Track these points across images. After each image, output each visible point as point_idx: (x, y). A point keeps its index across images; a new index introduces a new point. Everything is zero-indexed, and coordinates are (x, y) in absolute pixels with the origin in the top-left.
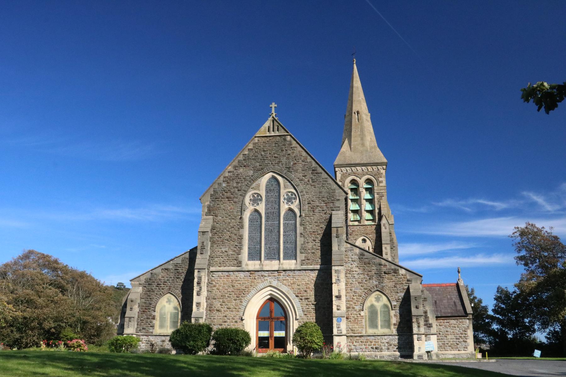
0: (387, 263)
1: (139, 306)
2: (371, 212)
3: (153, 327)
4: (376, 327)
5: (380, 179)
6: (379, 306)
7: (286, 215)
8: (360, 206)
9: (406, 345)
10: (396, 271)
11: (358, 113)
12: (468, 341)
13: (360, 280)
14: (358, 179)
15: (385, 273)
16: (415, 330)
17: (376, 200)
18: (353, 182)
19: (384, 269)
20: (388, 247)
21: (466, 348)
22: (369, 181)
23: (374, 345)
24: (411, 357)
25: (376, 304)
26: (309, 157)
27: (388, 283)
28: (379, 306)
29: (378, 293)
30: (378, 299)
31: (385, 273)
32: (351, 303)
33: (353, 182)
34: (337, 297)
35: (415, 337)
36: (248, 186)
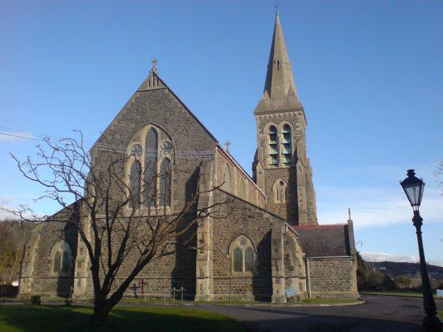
0: (252, 208)
1: (36, 252)
2: (287, 156)
3: (48, 270)
4: (241, 270)
5: (297, 124)
6: (243, 248)
7: (163, 163)
8: (278, 150)
9: (263, 288)
10: (260, 215)
11: (278, 62)
12: (351, 281)
13: (226, 224)
14: (276, 125)
15: (250, 217)
16: (274, 273)
17: (292, 144)
18: (273, 128)
19: (249, 213)
20: (303, 189)
21: (348, 288)
22: (286, 127)
23: (239, 287)
24: (269, 300)
25: (241, 247)
26: (184, 108)
27: (252, 226)
28: (243, 248)
29: (242, 236)
30: (243, 243)
31: (250, 217)
32: (218, 246)
33: (273, 128)
34: (200, 241)
35: (274, 280)
36: (130, 138)
